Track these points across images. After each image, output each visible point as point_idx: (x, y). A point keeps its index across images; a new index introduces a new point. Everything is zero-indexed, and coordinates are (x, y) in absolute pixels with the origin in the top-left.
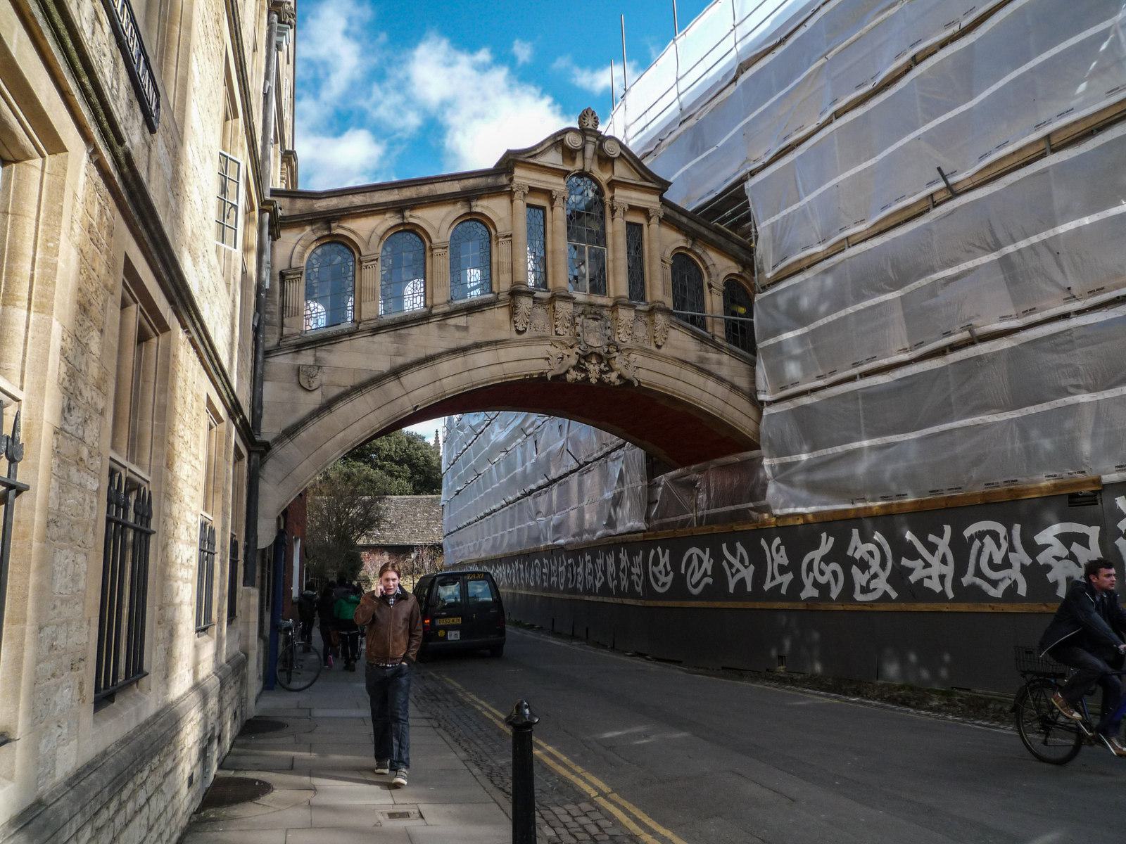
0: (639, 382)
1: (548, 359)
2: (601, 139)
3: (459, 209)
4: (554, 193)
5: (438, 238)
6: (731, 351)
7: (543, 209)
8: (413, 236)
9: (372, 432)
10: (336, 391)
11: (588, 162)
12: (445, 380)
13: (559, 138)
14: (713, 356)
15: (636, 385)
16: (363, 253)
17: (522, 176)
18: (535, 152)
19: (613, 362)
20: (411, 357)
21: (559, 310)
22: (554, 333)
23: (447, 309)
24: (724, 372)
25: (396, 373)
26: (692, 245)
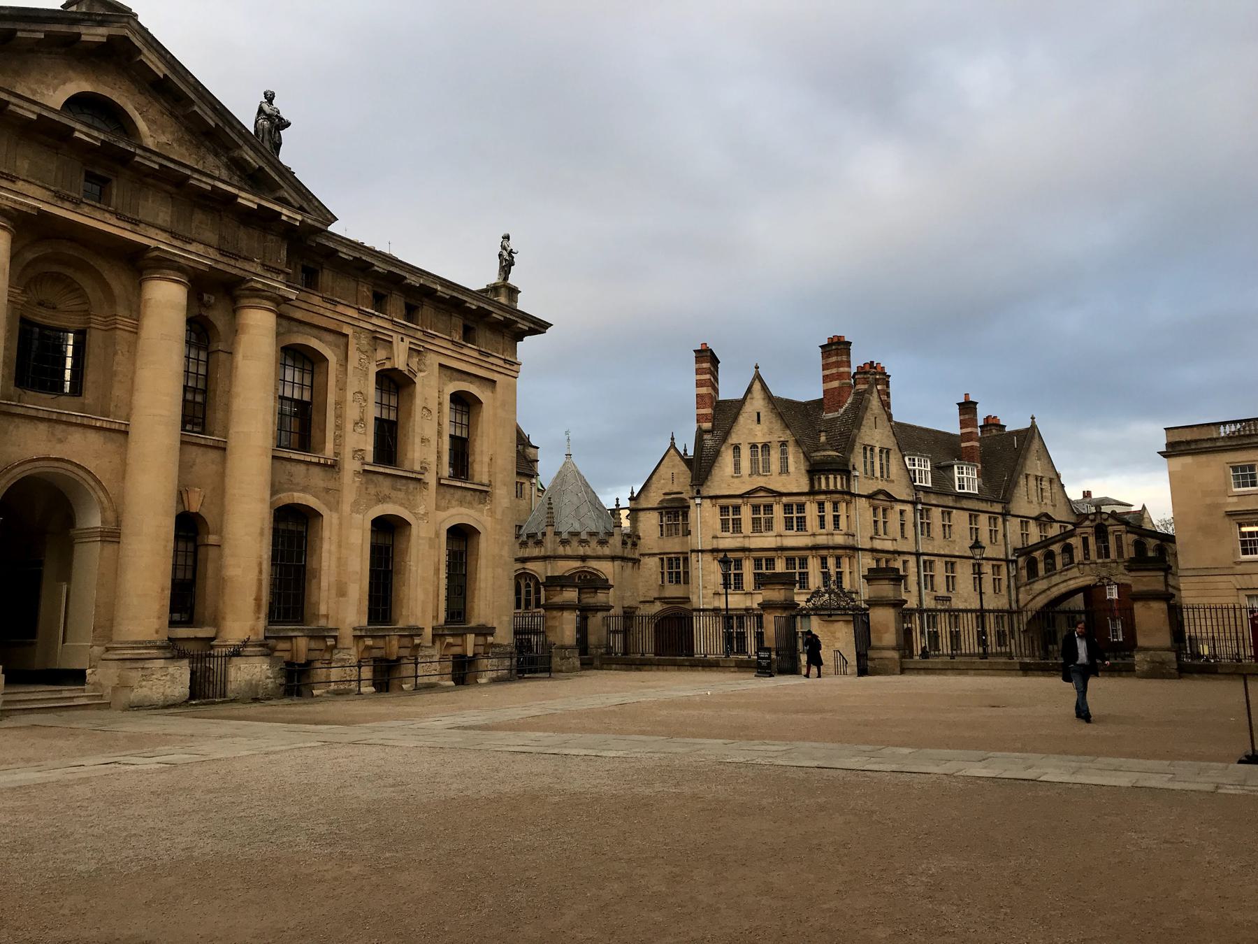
17: (1079, 530)
20: (1053, 583)
25: (1049, 589)
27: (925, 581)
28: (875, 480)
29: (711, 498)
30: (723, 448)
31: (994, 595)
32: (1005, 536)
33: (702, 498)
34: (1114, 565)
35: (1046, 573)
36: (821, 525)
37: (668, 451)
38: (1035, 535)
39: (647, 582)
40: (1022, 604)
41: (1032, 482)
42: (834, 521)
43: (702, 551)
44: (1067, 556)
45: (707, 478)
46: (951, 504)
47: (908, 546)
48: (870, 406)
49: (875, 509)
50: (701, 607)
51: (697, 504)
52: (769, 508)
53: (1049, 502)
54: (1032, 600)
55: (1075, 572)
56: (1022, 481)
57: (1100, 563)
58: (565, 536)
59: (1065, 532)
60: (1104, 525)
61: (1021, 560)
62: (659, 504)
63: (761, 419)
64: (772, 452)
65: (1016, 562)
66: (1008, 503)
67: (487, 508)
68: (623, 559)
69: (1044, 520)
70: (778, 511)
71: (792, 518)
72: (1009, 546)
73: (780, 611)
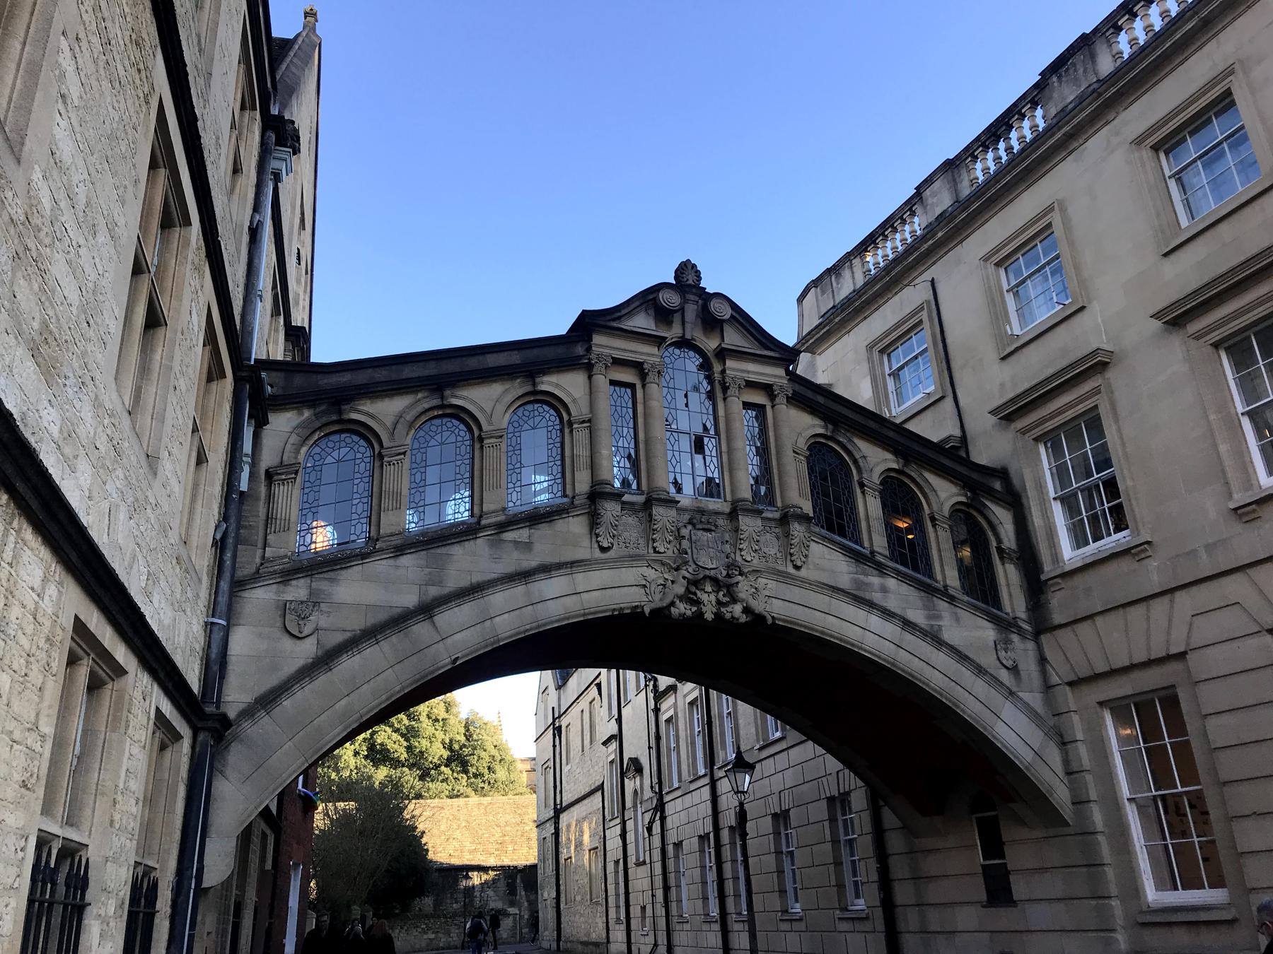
0: (773, 617)
1: (645, 586)
2: (706, 297)
3: (517, 388)
4: (646, 366)
5: (490, 423)
6: (898, 573)
7: (632, 386)
8: (456, 422)
9: (387, 699)
10: (338, 638)
11: (688, 326)
12: (497, 619)
13: (651, 297)
14: (875, 580)
15: (770, 621)
16: (385, 445)
17: (603, 343)
18: (619, 314)
19: (735, 589)
21: (658, 518)
22: (651, 551)
23: (501, 518)
24: (892, 604)
25: (426, 610)
26: (833, 431)
34: (748, 524)
57: (684, 510)
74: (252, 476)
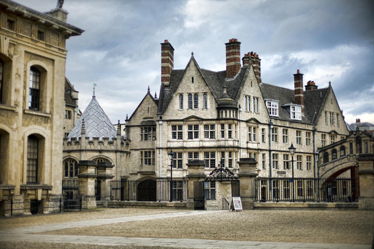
3: (340, 146)
10: (326, 171)
17: (348, 140)
25: (333, 168)
27: (273, 164)
28: (250, 113)
29: (167, 121)
30: (174, 95)
31: (306, 171)
32: (314, 141)
33: (163, 121)
35: (332, 160)
36: (222, 135)
37: (146, 96)
38: (328, 141)
39: (134, 163)
40: (320, 175)
41: (329, 115)
42: (229, 133)
43: (162, 148)
44: (342, 152)
45: (165, 111)
46: (288, 125)
47: (265, 146)
48: (249, 75)
49: (250, 128)
50: (161, 177)
51: (160, 124)
52: (196, 127)
53: (336, 124)
54: (325, 173)
55: (346, 160)
56: (323, 114)
58: (91, 139)
59: (343, 140)
60: (360, 137)
61: (321, 155)
62: (141, 123)
63: (194, 80)
64: (199, 98)
65: (318, 155)
66: (316, 125)
67: (48, 125)
68: (121, 152)
69: (333, 134)
70: (201, 129)
71: (208, 132)
72: (316, 146)
73: (196, 179)
74: (319, 158)
